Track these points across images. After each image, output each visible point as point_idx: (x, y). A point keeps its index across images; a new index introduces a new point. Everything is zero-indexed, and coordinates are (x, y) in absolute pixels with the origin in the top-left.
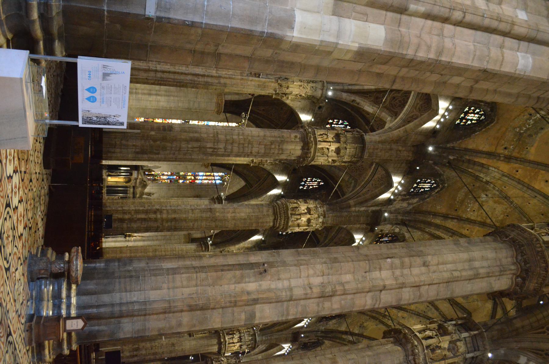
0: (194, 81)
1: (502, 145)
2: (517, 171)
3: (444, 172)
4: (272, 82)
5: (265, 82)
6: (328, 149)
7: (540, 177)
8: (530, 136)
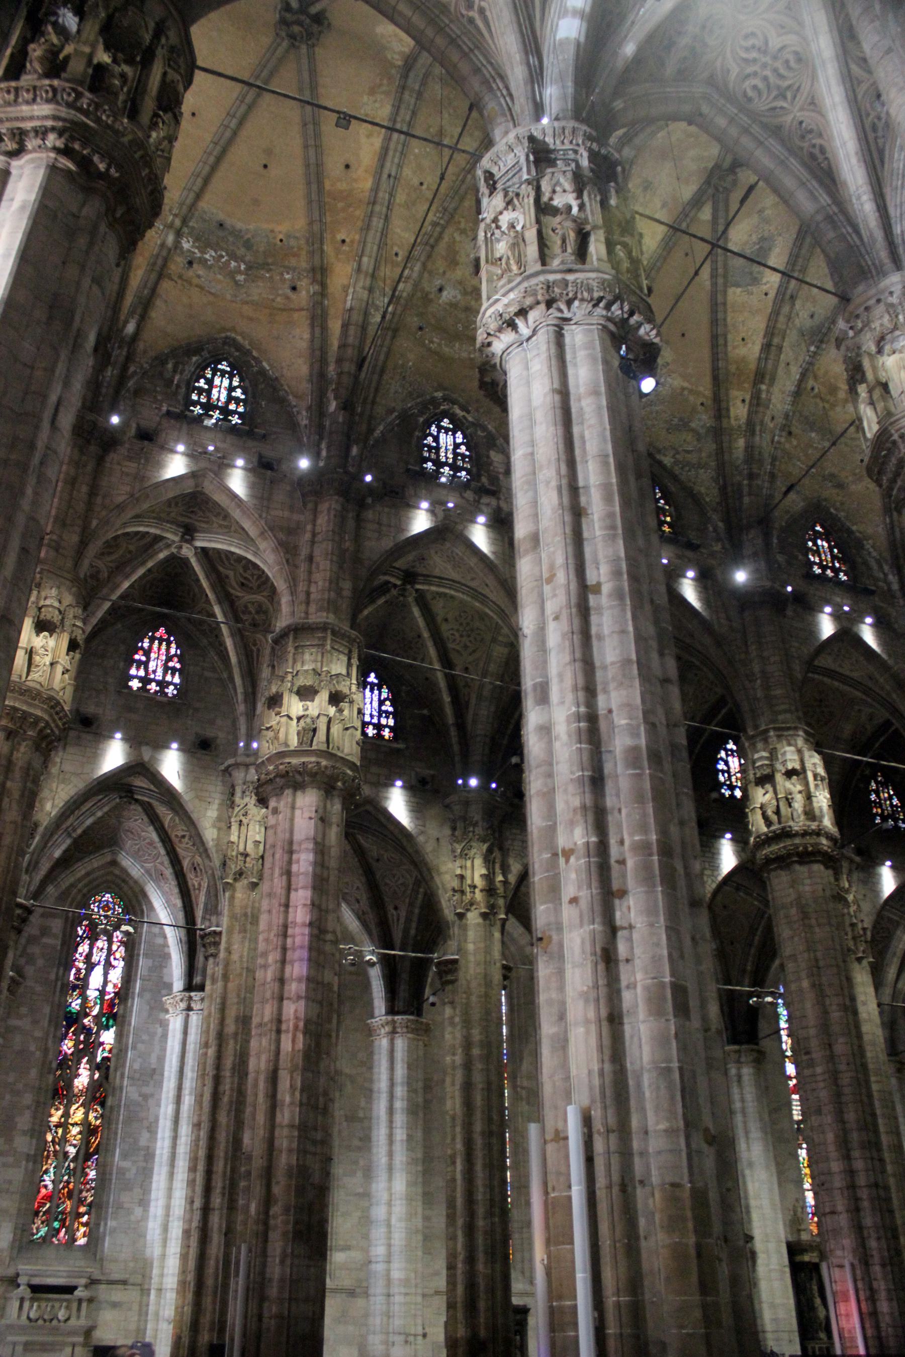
0: (231, 1102)
1: (288, 298)
2: (343, 241)
3: (390, 411)
4: (232, 897)
5: (233, 917)
6: (299, 719)
7: (342, 186)
8: (248, 245)
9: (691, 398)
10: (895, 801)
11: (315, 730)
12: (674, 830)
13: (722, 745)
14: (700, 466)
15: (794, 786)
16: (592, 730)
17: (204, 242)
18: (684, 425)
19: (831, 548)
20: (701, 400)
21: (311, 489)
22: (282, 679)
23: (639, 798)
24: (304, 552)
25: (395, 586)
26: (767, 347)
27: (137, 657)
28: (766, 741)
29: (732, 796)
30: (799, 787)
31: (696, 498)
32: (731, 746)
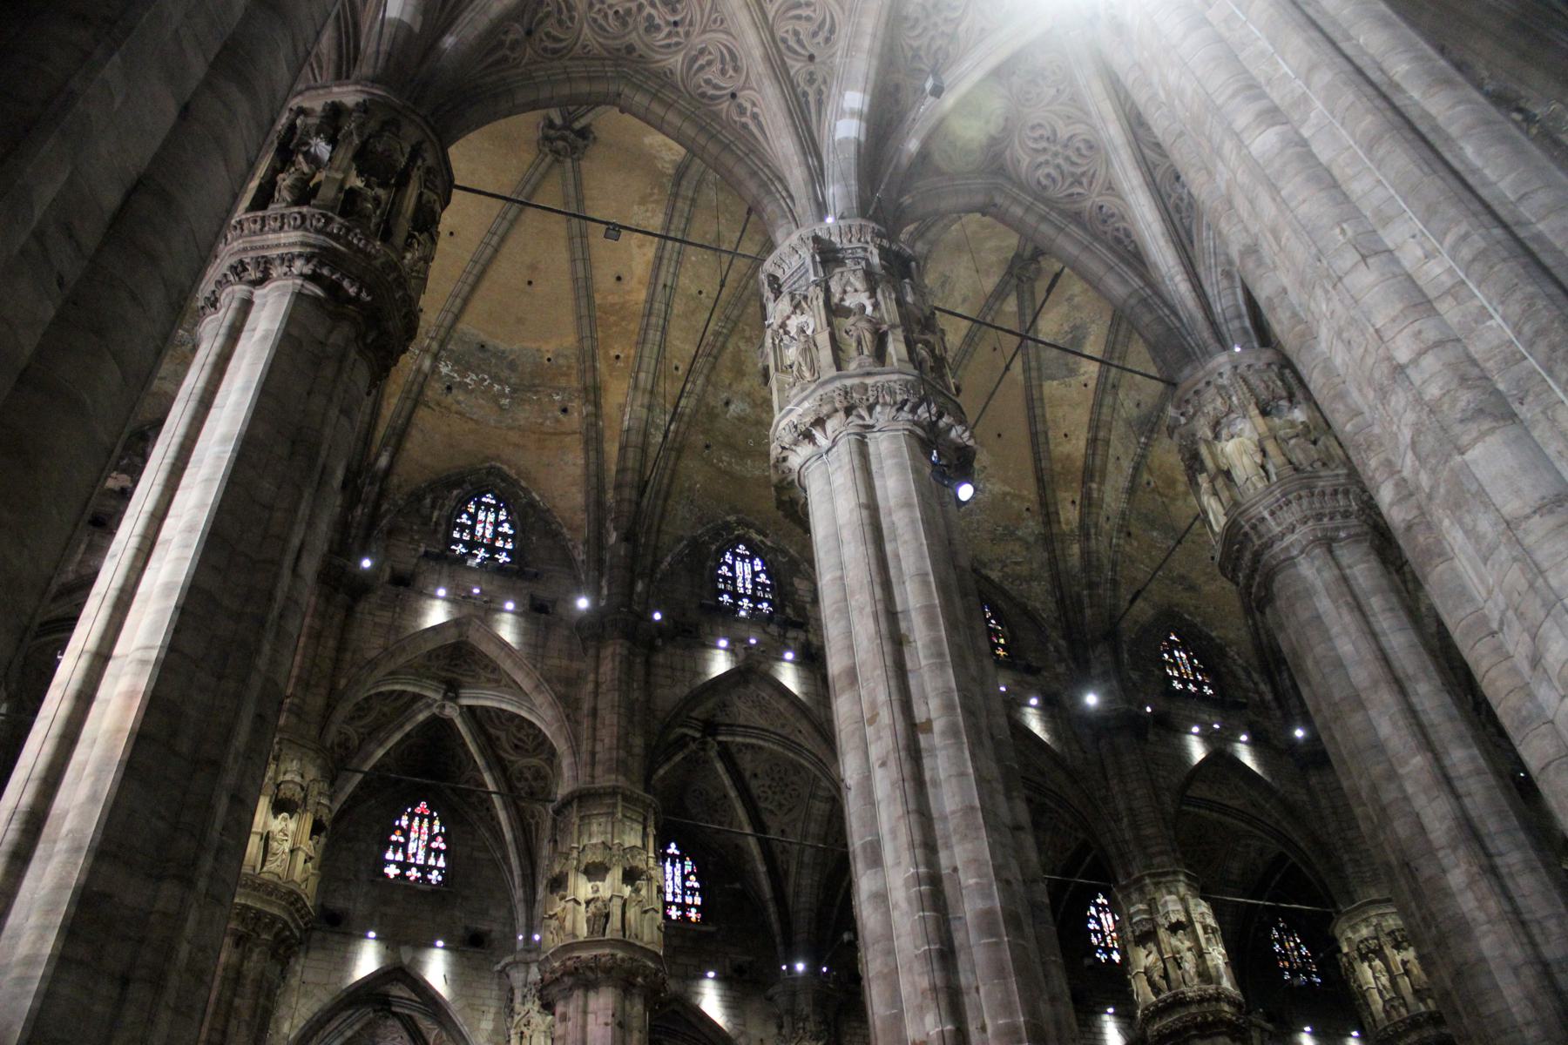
1: (557, 421)
2: (618, 357)
3: (680, 539)
6: (588, 903)
8: (512, 366)
9: (1015, 504)
10: (1304, 951)
11: (607, 916)
12: (1045, 1009)
13: (1090, 899)
14: (1031, 578)
15: (1182, 943)
16: (935, 893)
17: (463, 365)
18: (1010, 534)
19: (1190, 659)
20: (1027, 505)
21: (592, 631)
22: (567, 856)
23: (1000, 973)
24: (586, 707)
25: (694, 739)
26: (1093, 442)
27: (394, 838)
28: (1141, 890)
29: (1110, 960)
30: (1188, 944)
31: (1031, 616)
32: (1101, 900)
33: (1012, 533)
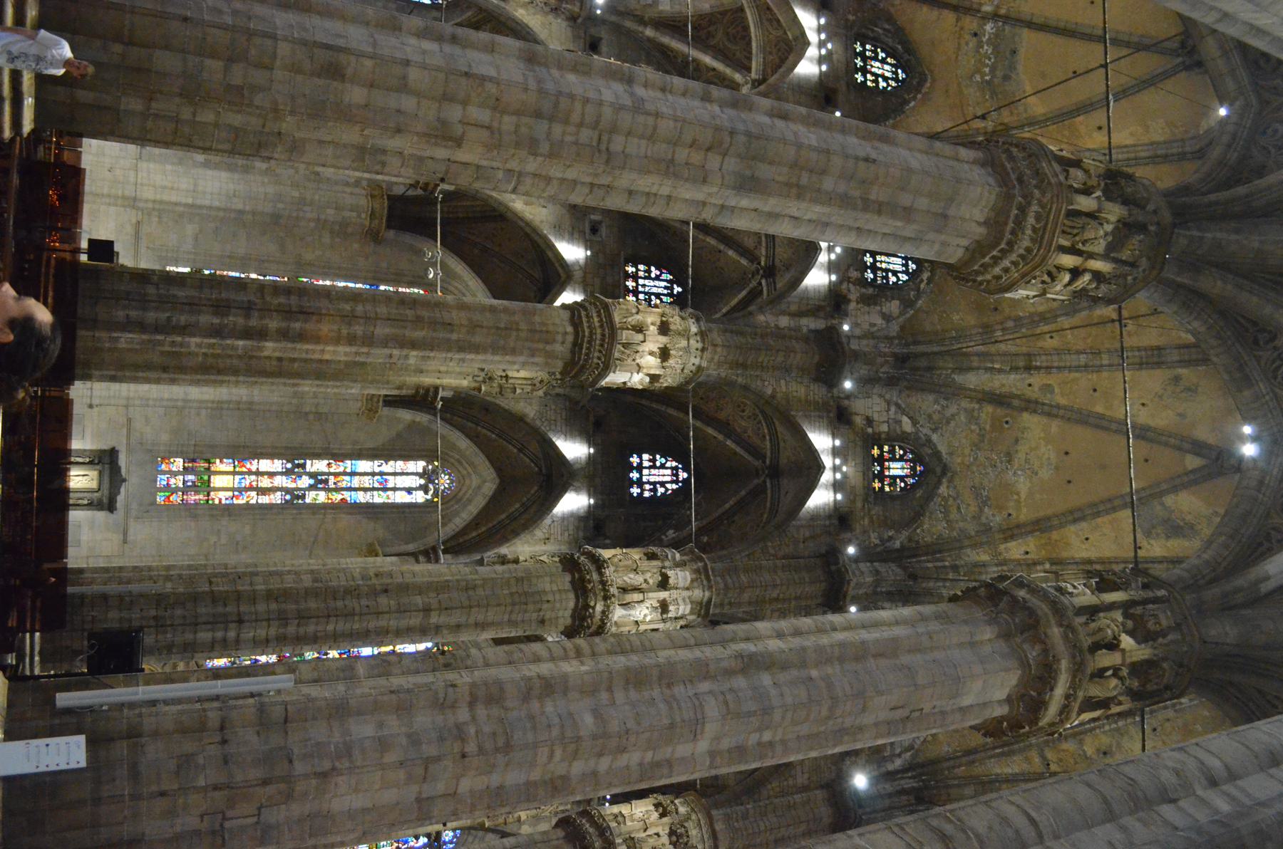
7: (1082, 129)
8: (1006, 78)
9: (1012, 504)
17: (996, 40)
27: (653, 268)
31: (917, 516)
33: (985, 503)
